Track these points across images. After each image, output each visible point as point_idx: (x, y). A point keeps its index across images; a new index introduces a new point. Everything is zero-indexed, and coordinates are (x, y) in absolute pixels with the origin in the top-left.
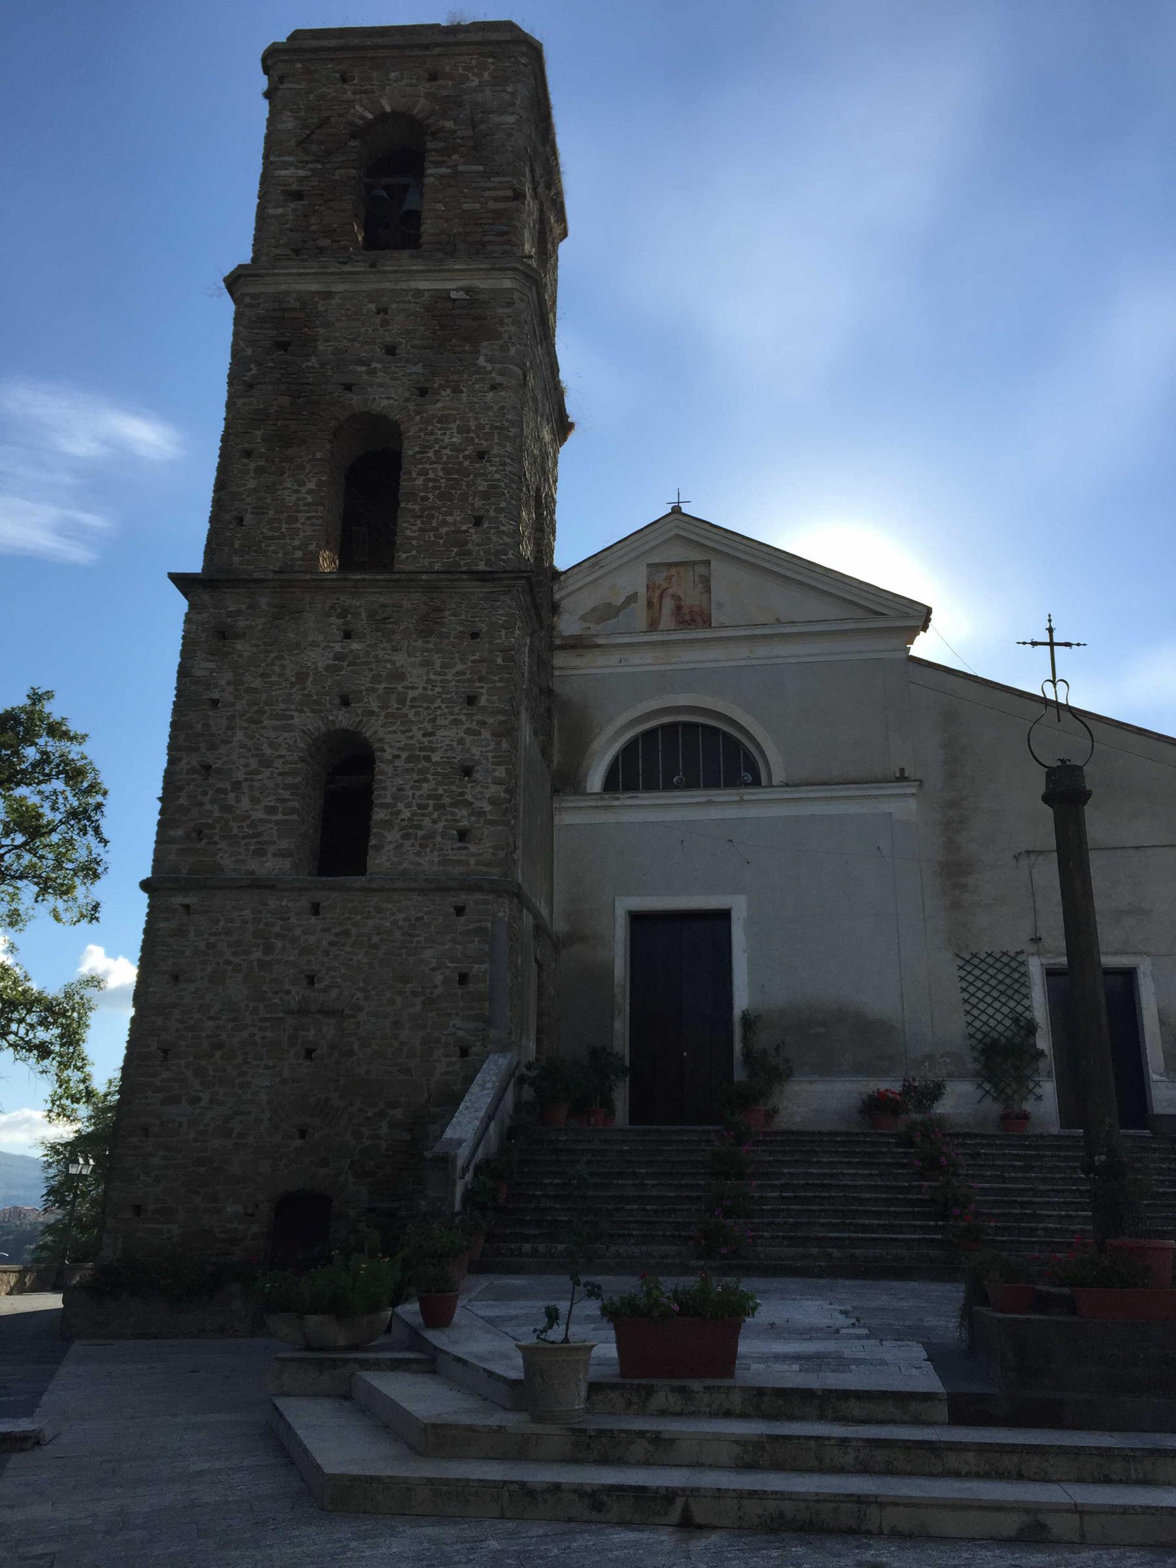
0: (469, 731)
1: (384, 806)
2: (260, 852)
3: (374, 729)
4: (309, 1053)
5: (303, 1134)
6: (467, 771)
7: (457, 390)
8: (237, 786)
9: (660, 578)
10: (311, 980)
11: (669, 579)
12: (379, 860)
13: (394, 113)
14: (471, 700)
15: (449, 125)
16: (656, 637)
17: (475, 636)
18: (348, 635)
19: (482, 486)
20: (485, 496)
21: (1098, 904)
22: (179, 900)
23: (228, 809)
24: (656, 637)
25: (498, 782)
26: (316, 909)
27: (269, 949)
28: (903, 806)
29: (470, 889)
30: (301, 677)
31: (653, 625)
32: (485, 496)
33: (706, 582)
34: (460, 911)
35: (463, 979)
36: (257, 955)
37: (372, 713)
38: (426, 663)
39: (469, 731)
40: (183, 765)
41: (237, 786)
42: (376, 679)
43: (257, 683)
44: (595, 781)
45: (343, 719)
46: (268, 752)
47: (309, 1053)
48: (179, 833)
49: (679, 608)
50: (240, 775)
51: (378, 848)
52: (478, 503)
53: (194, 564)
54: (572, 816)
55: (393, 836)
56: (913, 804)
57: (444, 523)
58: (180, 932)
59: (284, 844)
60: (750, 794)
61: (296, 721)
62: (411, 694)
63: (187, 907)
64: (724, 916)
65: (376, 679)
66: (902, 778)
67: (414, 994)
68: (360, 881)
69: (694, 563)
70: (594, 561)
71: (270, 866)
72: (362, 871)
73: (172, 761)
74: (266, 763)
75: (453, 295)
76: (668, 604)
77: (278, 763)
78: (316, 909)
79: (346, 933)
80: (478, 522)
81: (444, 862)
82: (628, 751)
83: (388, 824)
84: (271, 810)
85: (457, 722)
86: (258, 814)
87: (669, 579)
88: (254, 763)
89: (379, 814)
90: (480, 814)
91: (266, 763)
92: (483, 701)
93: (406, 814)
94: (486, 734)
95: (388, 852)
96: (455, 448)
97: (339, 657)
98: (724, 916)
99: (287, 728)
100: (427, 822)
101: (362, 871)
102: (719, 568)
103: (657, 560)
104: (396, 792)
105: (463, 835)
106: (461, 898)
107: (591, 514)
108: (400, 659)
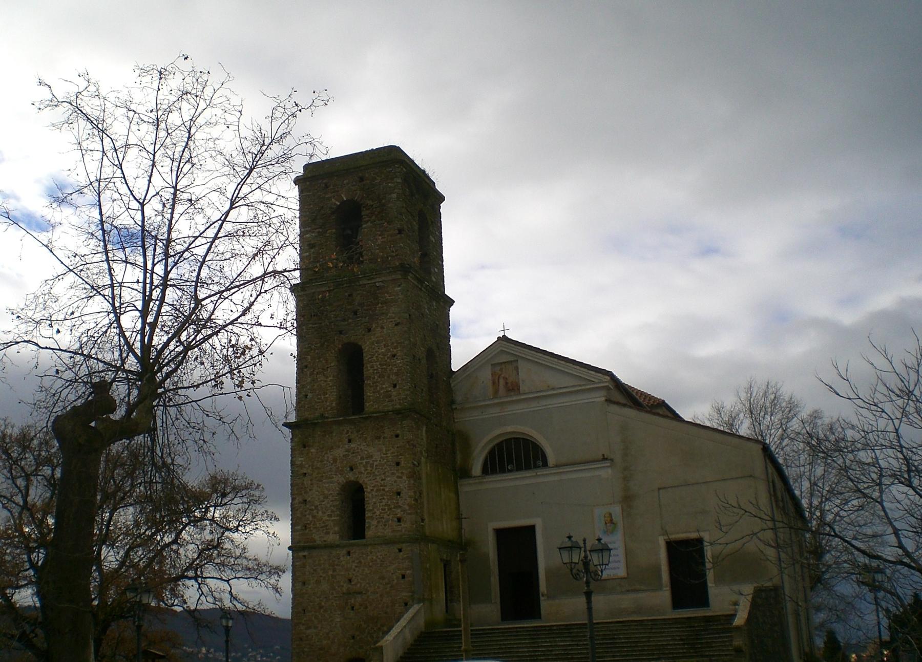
0: (398, 477)
1: (370, 511)
2: (327, 533)
3: (364, 479)
4: (353, 608)
5: (353, 637)
6: (399, 494)
7: (382, 328)
8: (316, 507)
9: (498, 368)
10: (350, 581)
11: (501, 370)
12: (369, 533)
13: (347, 200)
14: (398, 464)
15: (370, 202)
16: (496, 401)
17: (397, 436)
18: (350, 441)
19: (395, 370)
20: (397, 374)
21: (499, 607)
22: (301, 554)
23: (314, 517)
24: (496, 401)
25: (410, 497)
26: (349, 553)
27: (334, 570)
28: (606, 472)
29: (403, 543)
30: (335, 460)
31: (496, 392)
32: (397, 374)
33: (517, 369)
34: (400, 550)
35: (403, 577)
36: (330, 573)
37: (362, 473)
38: (380, 450)
39: (398, 477)
40: (296, 501)
41: (316, 507)
42: (362, 458)
43: (319, 465)
44: (477, 469)
45: (351, 477)
46: (326, 492)
47: (353, 608)
48: (299, 527)
49: (507, 383)
50: (317, 503)
51: (369, 527)
52: (394, 377)
53: (292, 418)
54: (467, 487)
55: (375, 522)
56: (610, 470)
57: (382, 388)
58: (304, 566)
59: (336, 529)
60: (540, 472)
61: (335, 479)
62: (375, 463)
63: (305, 556)
64: (532, 528)
65: (362, 458)
66: (604, 459)
67: (387, 584)
68: (363, 541)
69: (511, 362)
70: (465, 367)
71: (333, 538)
72: (364, 537)
73: (293, 499)
74: (326, 497)
75: (377, 284)
76: (502, 382)
77: (330, 497)
78: (349, 553)
79: (360, 562)
80: (395, 386)
81: (393, 531)
82: (491, 453)
83: (372, 518)
84: (330, 516)
85: (393, 474)
86: (326, 518)
87: (501, 370)
88: (321, 498)
89: (368, 514)
90: (404, 511)
91: (326, 497)
92: (402, 464)
93: (378, 513)
94: (404, 478)
95: (373, 529)
96: (384, 355)
97: (348, 451)
98: (532, 528)
99: (331, 482)
100: (385, 516)
101: (364, 537)
102: (521, 364)
103: (496, 361)
104: (374, 504)
105: (399, 520)
106: (399, 546)
107: (464, 348)
108: (371, 450)
